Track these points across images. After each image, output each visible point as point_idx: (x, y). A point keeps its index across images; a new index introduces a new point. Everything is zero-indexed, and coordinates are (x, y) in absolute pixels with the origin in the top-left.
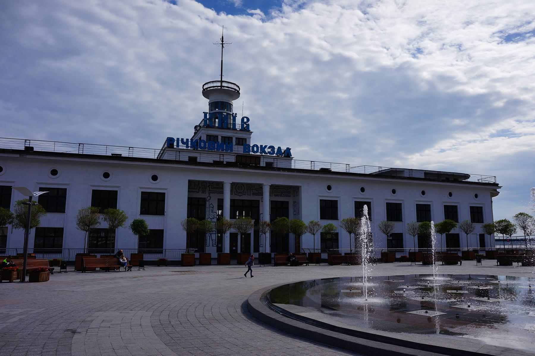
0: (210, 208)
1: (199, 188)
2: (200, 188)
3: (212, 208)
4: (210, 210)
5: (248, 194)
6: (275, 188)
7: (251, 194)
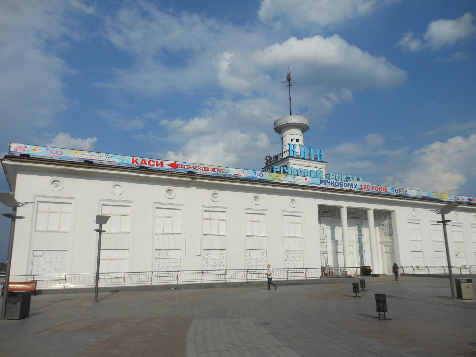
4: (322, 232)
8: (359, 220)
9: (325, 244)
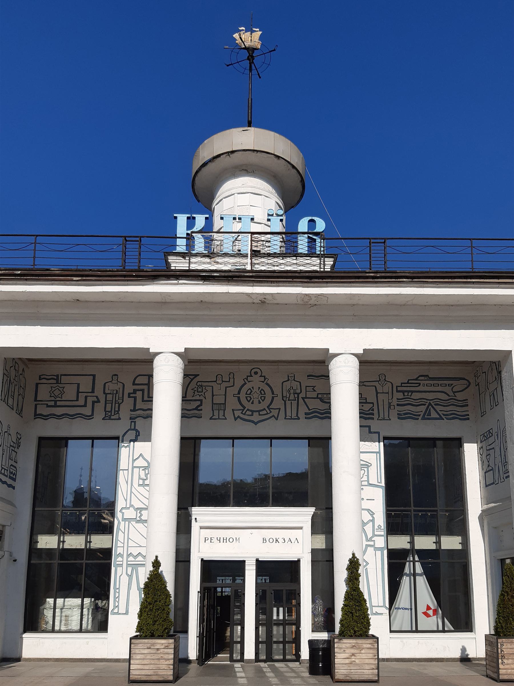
1: (94, 403)
2: (98, 401)
5: (289, 414)
6: (398, 391)
7: (301, 415)
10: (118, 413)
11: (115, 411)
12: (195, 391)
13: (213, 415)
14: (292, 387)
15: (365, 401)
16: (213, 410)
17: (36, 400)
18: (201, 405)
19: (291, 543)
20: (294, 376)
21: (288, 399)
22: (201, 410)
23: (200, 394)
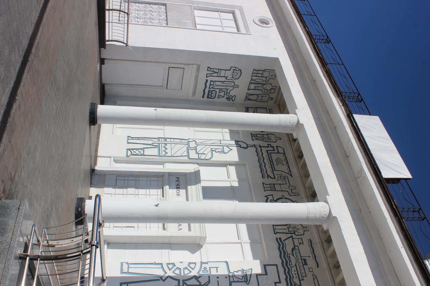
0: (221, 147)
3: (220, 150)
5: (277, 227)
7: (278, 236)
8: (283, 277)
9: (185, 154)
10: (256, 140)
11: (258, 138)
12: (281, 175)
13: (266, 184)
14: (298, 230)
15: (301, 279)
16: (269, 184)
17: (256, 108)
18: (271, 178)
19: (178, 226)
20: (308, 231)
21: (289, 227)
22: (268, 178)
23: (279, 177)
